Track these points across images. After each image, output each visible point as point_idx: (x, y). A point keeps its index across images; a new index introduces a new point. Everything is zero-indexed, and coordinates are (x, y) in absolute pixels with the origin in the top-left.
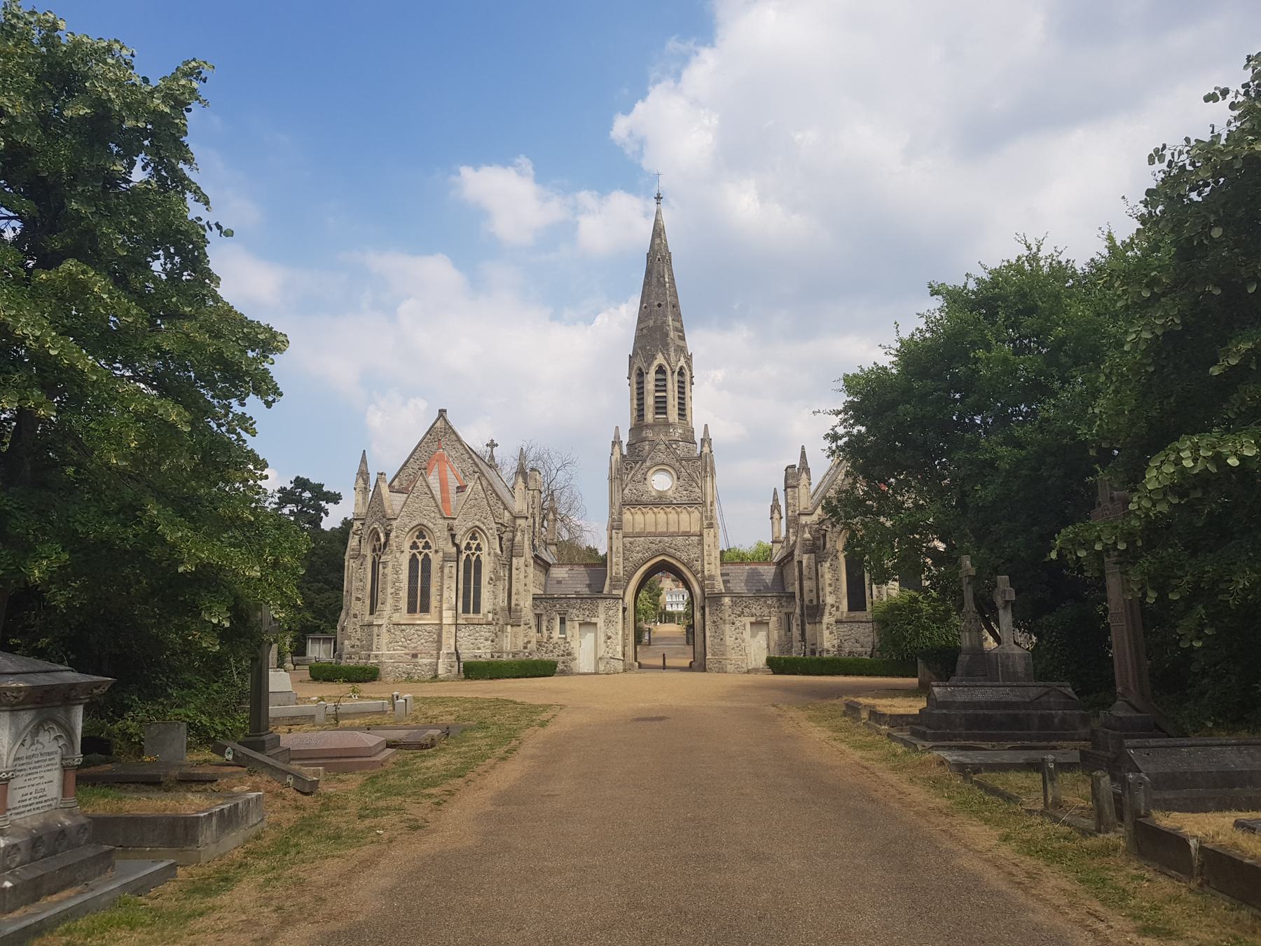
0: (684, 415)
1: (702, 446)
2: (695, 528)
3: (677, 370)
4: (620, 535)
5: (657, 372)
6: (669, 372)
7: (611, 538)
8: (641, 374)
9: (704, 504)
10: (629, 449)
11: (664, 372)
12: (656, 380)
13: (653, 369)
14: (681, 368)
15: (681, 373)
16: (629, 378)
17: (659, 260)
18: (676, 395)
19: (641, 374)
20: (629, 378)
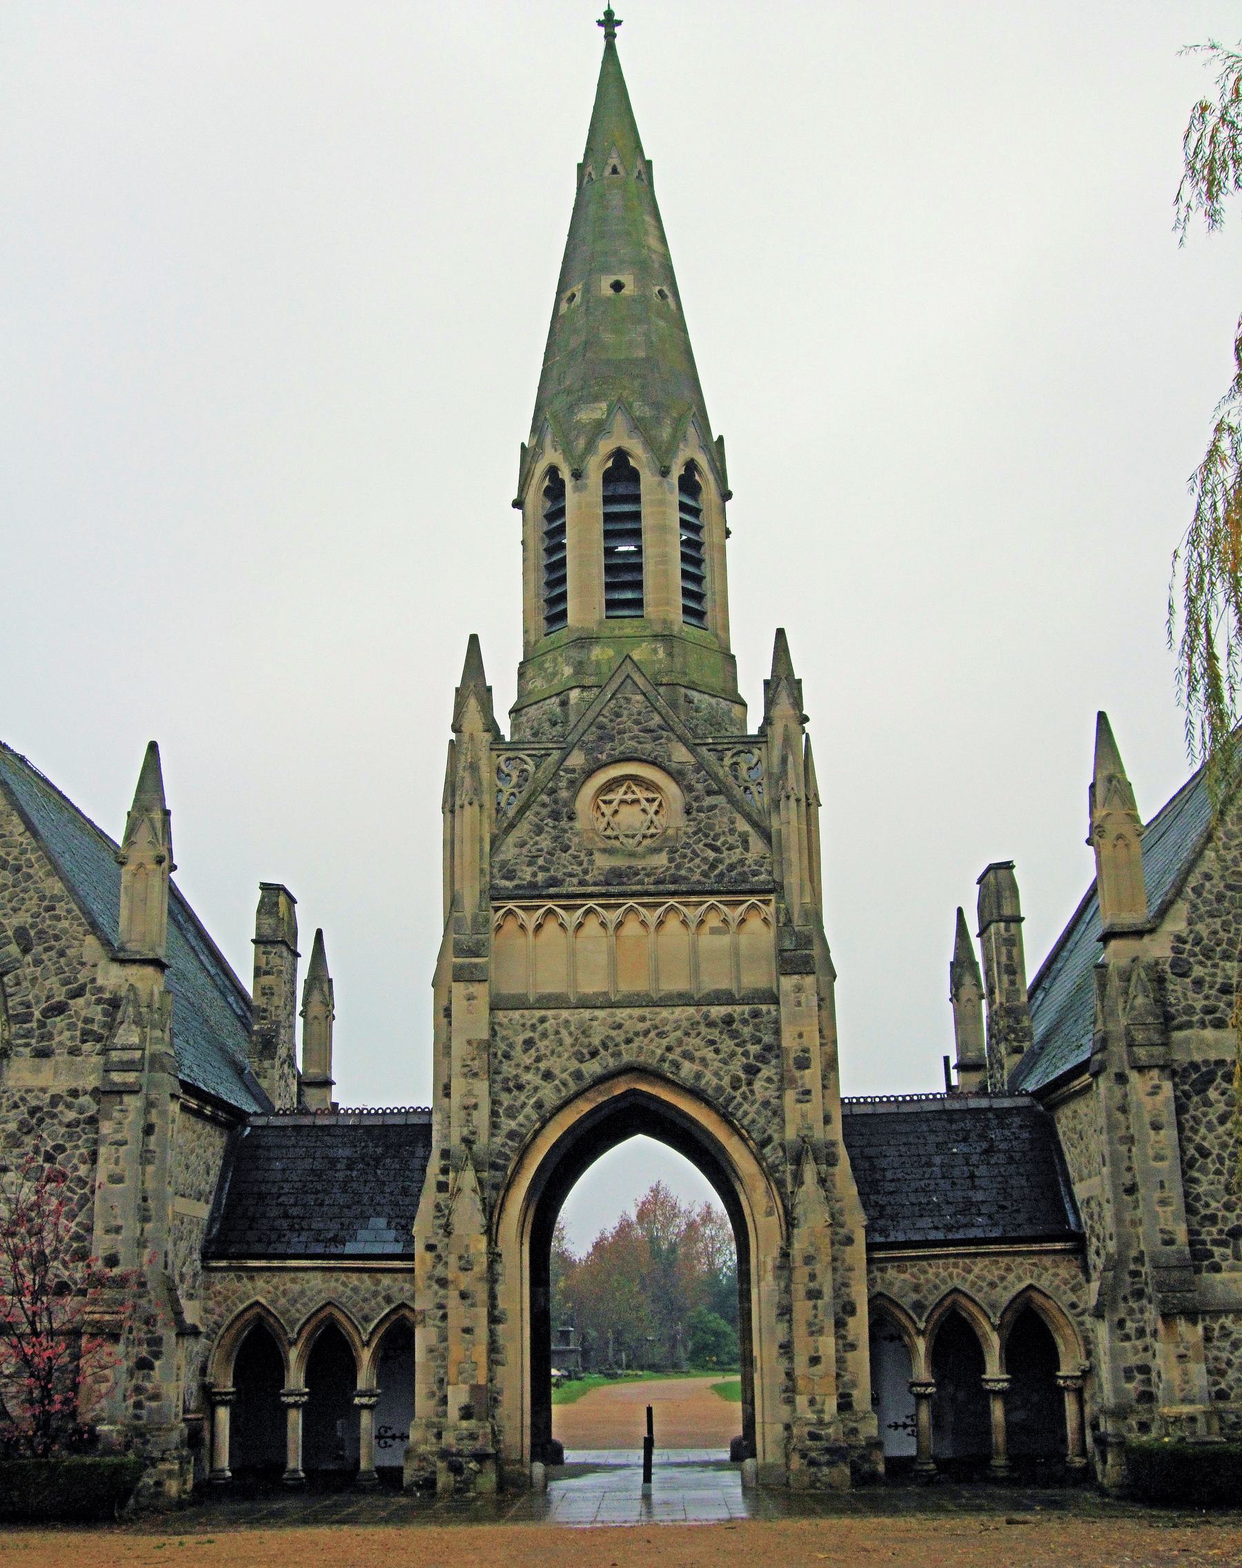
0: (700, 615)
1: (769, 703)
2: (757, 977)
3: (677, 471)
4: (483, 1004)
5: (608, 477)
6: (648, 479)
7: (448, 1013)
8: (555, 491)
9: (777, 888)
10: (515, 727)
11: (634, 476)
12: (607, 500)
13: (596, 467)
14: (691, 466)
15: (689, 485)
16: (518, 504)
17: (615, 171)
18: (677, 566)
19: (555, 491)
20: (518, 504)
